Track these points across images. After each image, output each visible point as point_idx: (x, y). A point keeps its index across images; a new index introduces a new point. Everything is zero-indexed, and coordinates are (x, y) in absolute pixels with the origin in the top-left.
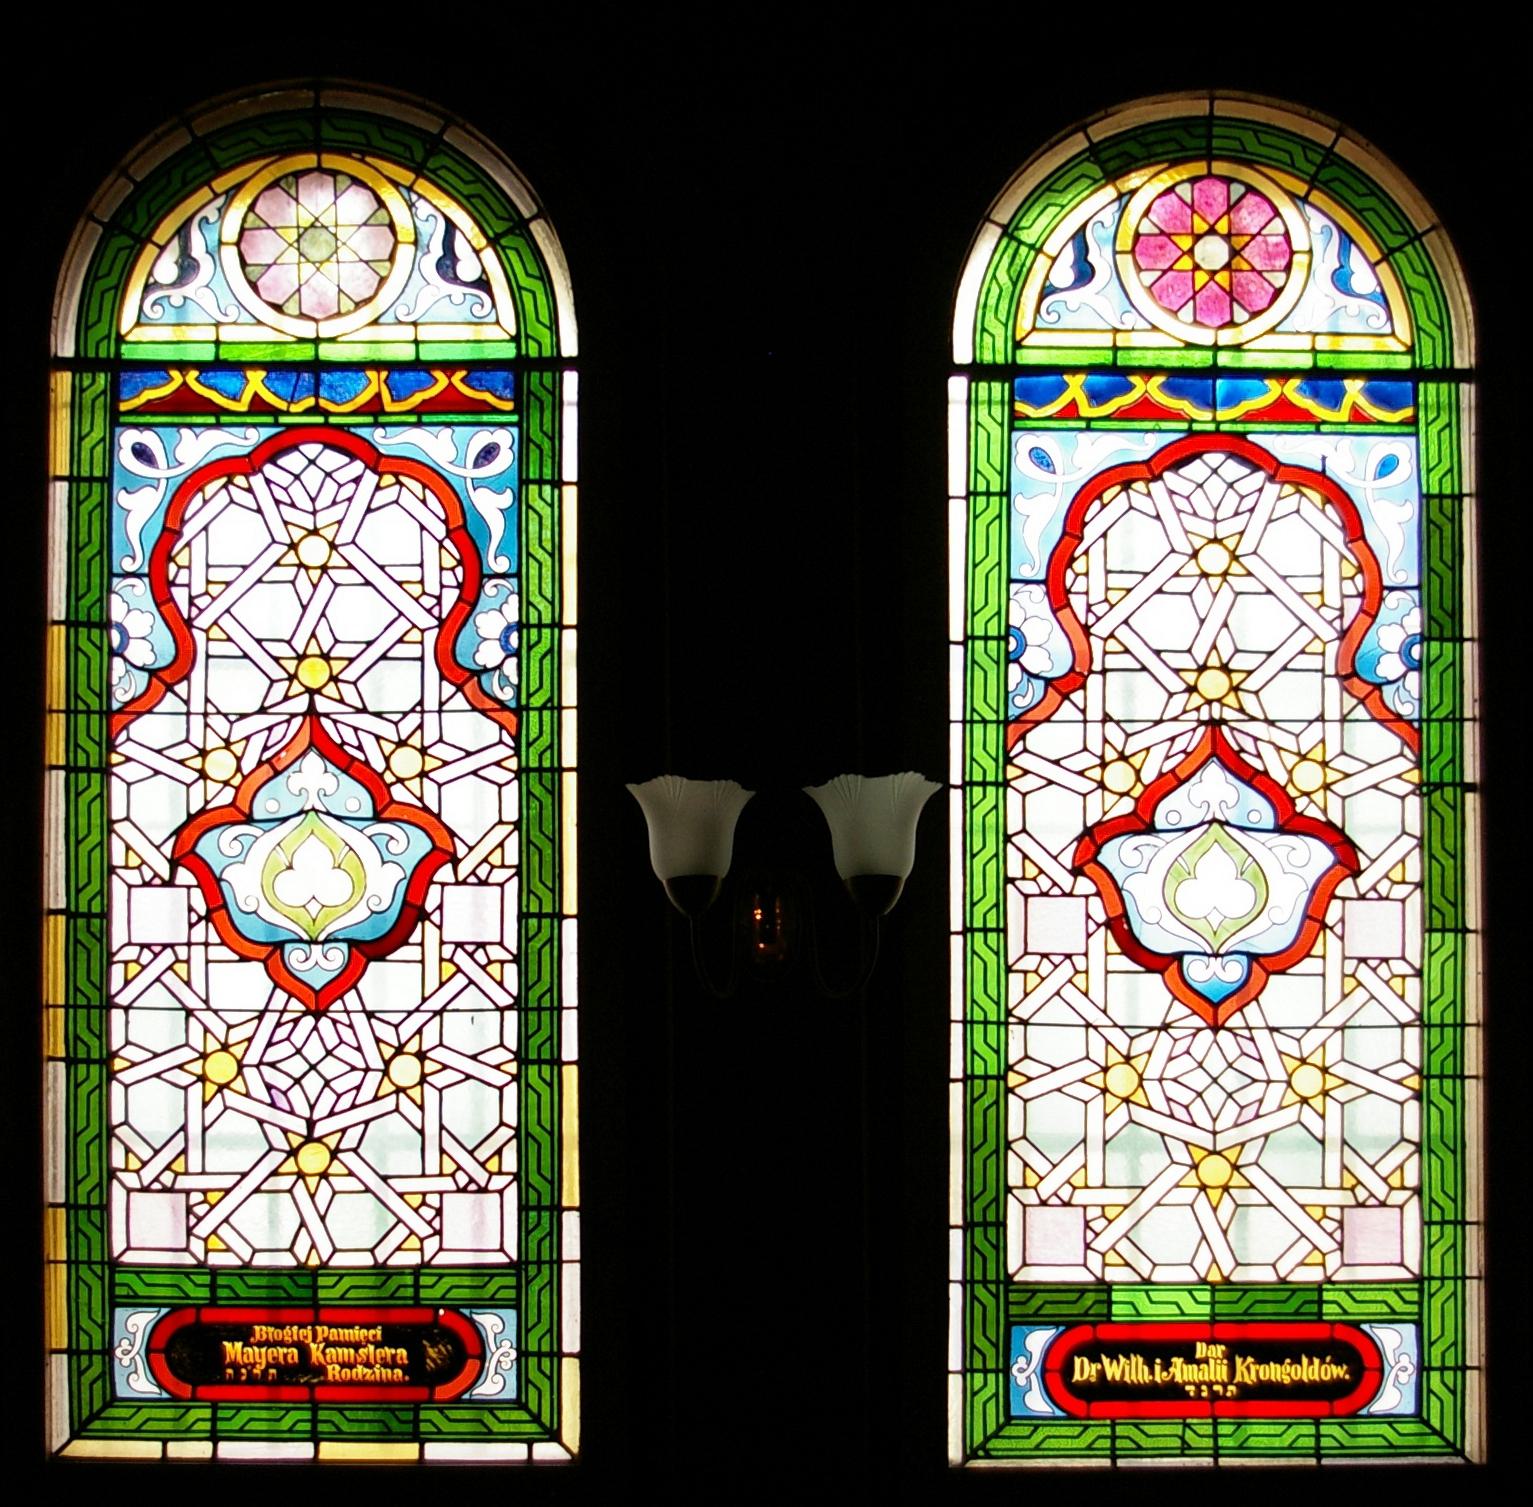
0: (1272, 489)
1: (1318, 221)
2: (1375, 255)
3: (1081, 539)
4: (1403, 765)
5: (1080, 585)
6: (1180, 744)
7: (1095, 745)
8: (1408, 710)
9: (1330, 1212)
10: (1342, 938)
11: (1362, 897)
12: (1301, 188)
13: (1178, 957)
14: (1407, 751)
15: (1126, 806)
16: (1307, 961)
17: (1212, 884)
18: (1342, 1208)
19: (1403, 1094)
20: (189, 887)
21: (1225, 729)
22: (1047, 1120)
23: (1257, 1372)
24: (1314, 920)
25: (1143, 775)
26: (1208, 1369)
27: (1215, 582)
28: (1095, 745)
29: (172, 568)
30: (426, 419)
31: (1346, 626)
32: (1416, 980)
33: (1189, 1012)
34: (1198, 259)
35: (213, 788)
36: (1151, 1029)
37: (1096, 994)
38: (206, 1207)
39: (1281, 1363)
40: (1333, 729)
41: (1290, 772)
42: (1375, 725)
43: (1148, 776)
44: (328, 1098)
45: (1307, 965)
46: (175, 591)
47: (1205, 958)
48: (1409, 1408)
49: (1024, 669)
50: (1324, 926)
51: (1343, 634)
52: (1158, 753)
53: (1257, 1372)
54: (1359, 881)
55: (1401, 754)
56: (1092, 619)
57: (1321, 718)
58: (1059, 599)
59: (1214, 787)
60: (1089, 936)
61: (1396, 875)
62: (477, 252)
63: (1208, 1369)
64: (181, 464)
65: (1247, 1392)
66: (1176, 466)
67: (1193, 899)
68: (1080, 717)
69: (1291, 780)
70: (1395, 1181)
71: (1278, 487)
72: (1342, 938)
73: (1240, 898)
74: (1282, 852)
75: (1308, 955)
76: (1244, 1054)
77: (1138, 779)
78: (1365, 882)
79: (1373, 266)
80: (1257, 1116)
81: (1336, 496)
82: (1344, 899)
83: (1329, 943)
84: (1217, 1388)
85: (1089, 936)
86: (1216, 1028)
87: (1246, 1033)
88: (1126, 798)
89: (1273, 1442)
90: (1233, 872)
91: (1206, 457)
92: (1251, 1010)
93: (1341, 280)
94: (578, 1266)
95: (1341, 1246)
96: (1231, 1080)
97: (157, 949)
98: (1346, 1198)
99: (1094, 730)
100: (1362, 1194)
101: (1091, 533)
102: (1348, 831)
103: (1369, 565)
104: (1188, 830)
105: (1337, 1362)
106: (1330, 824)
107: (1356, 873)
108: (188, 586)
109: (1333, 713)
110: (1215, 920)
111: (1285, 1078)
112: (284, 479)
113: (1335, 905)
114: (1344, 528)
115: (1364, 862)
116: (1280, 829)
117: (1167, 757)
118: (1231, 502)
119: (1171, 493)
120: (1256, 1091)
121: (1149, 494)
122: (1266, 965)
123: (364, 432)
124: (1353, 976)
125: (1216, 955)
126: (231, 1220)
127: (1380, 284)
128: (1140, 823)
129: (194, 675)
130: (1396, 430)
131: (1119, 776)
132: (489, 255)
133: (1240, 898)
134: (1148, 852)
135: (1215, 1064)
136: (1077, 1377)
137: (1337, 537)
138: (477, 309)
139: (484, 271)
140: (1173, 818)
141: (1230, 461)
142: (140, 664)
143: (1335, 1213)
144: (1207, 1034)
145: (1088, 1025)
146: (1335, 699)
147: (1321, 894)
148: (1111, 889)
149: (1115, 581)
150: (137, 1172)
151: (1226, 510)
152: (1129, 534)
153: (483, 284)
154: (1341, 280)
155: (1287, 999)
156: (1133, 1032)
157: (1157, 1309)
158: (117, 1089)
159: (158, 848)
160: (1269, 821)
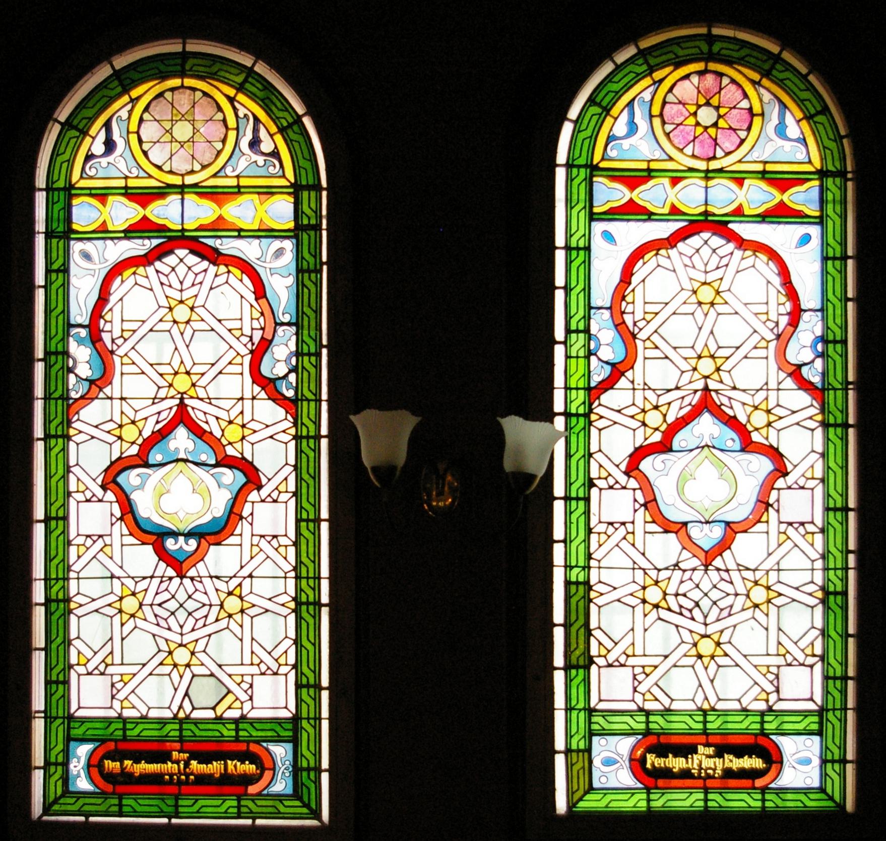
0: (738, 254)
1: (767, 97)
2: (799, 115)
3: (630, 283)
4: (813, 411)
5: (108, 327)
6: (687, 401)
7: (639, 402)
8: (816, 380)
9: (771, 669)
10: (251, 524)
11: (263, 501)
12: (756, 77)
13: (685, 524)
14: (815, 403)
15: (657, 437)
16: (232, 537)
17: (181, 495)
18: (779, 667)
19: (812, 601)
20: (634, 490)
21: (713, 394)
22: (88, 631)
23: (687, 763)
24: (763, 504)
25: (143, 433)
26: (703, 760)
27: (706, 307)
28: (639, 402)
29: (102, 322)
30: (129, 235)
31: (780, 331)
32: (820, 535)
33: (691, 555)
34: (699, 119)
35: (125, 445)
36: (144, 578)
37: (117, 557)
38: (122, 684)
39: (750, 757)
40: (248, 403)
41: (223, 431)
42: (270, 402)
43: (671, 419)
44: (191, 621)
45: (232, 540)
46: (103, 334)
47: (700, 524)
48: (289, 791)
49: (76, 375)
50: (241, 518)
51: (778, 337)
52: (675, 406)
53: (687, 763)
54: (261, 492)
55: (812, 405)
56: (115, 347)
57: (242, 399)
58: (95, 336)
59: (706, 425)
60: (112, 525)
61: (809, 475)
62: (271, 136)
63: (703, 760)
64: (107, 261)
65: (729, 773)
66: (159, 258)
67: (168, 504)
68: (631, 386)
69: (749, 421)
70: (809, 651)
71: (741, 252)
72: (251, 524)
73: (722, 491)
74: (744, 464)
75: (232, 534)
76: (722, 579)
77: (665, 421)
78: (264, 492)
79: (798, 122)
80: (730, 615)
81: (773, 255)
82: (779, 489)
83: (244, 528)
84: (709, 771)
85: (112, 525)
86: (182, 576)
87: (199, 579)
88: (134, 445)
89: (743, 801)
90: (717, 475)
91: (701, 234)
92: (200, 565)
93: (781, 130)
94: (556, 707)
95: (251, 699)
96: (715, 595)
97: (95, 538)
98: (780, 661)
99: (639, 394)
100: (789, 659)
101: (635, 280)
102: (255, 463)
103: (792, 294)
104: (691, 450)
105: (251, 763)
106: (771, 446)
107: (259, 487)
108: (111, 331)
109: (248, 395)
110: (181, 515)
111: (745, 592)
112: (166, 270)
113: (774, 493)
114: (779, 274)
115: (264, 480)
116: (743, 450)
117: (681, 408)
118: (715, 261)
119: (157, 271)
120: (729, 600)
121: (669, 257)
122: (732, 529)
123: (210, 242)
124: (784, 533)
125: (707, 522)
126: (136, 691)
127: (802, 133)
128: (664, 446)
129: (114, 381)
130: (754, 219)
131: (130, 433)
132: (279, 138)
133: (722, 491)
134: (668, 464)
135: (706, 585)
136: (649, 766)
137: (777, 281)
138: (271, 169)
139: (276, 147)
140: (683, 444)
141: (191, 256)
142: (84, 377)
143: (248, 679)
144: (177, 581)
145: (112, 577)
146: (250, 388)
147: (768, 486)
148: (646, 485)
149: (649, 308)
150: (85, 665)
151: (187, 283)
152: (658, 282)
153: (275, 154)
154: (781, 130)
155: (222, 559)
156: (137, 579)
157: (678, 724)
158: (73, 618)
159: (94, 480)
160: (737, 446)
